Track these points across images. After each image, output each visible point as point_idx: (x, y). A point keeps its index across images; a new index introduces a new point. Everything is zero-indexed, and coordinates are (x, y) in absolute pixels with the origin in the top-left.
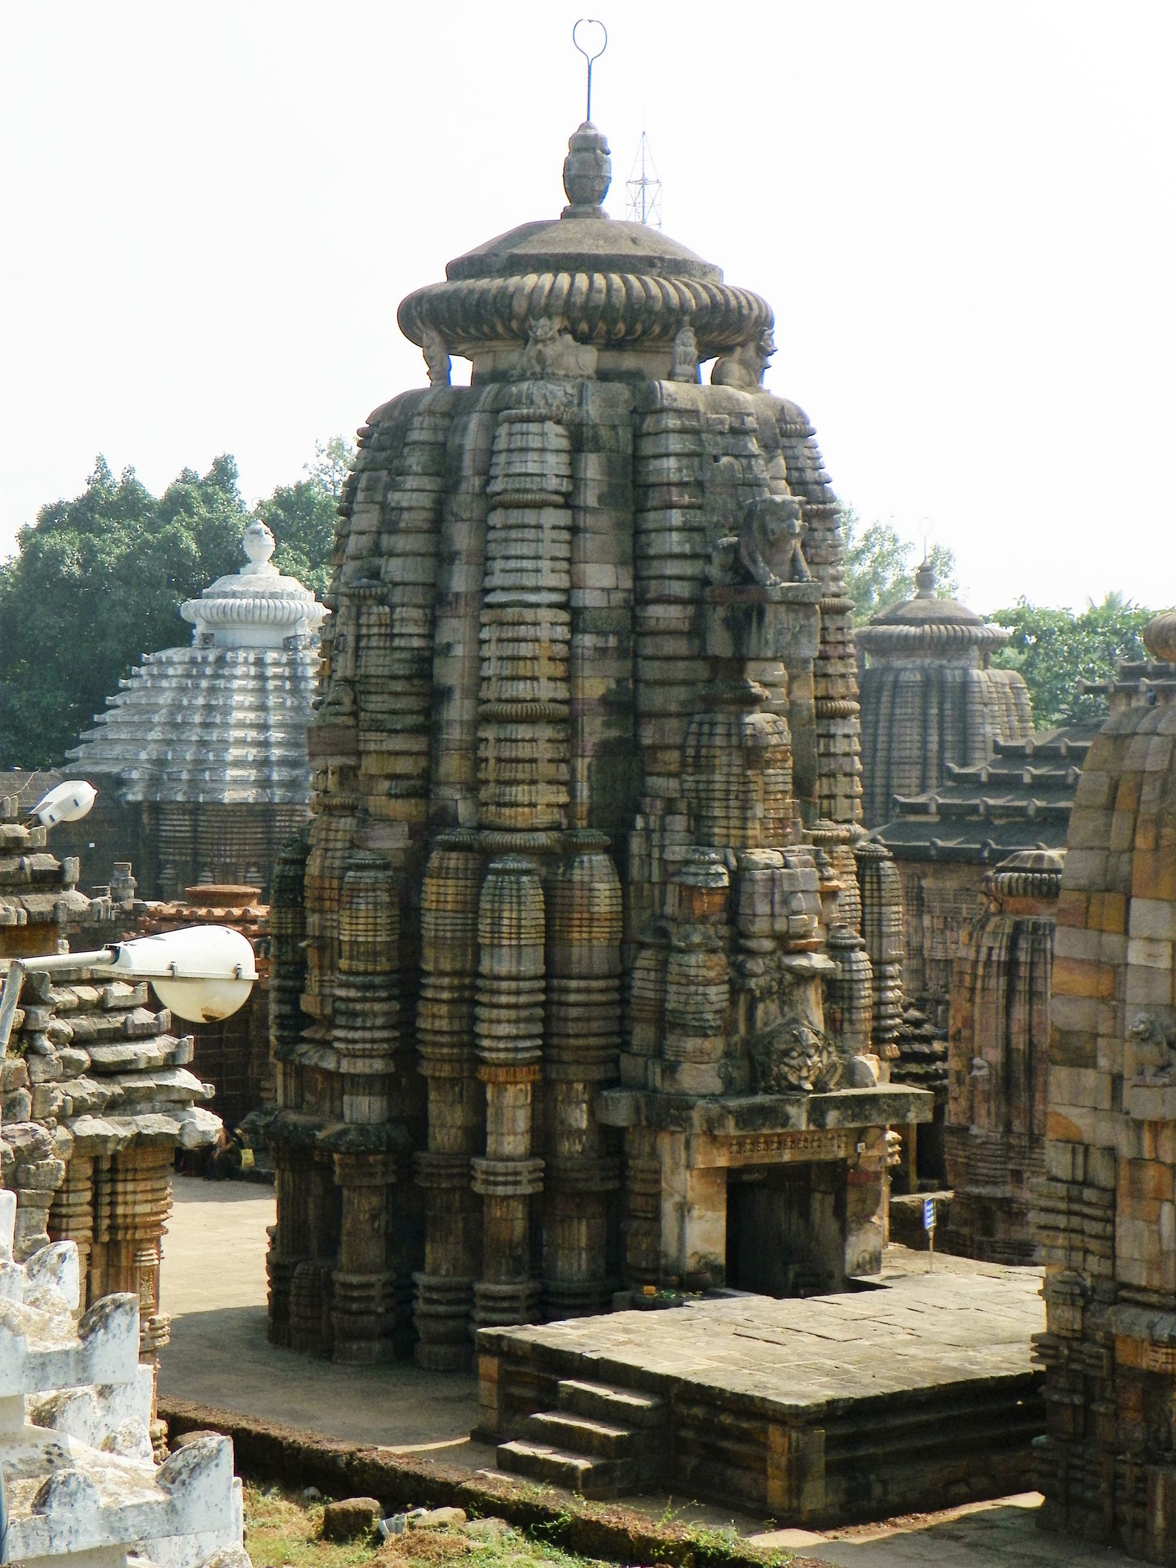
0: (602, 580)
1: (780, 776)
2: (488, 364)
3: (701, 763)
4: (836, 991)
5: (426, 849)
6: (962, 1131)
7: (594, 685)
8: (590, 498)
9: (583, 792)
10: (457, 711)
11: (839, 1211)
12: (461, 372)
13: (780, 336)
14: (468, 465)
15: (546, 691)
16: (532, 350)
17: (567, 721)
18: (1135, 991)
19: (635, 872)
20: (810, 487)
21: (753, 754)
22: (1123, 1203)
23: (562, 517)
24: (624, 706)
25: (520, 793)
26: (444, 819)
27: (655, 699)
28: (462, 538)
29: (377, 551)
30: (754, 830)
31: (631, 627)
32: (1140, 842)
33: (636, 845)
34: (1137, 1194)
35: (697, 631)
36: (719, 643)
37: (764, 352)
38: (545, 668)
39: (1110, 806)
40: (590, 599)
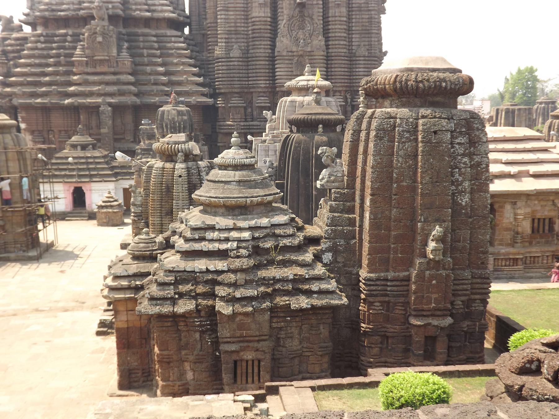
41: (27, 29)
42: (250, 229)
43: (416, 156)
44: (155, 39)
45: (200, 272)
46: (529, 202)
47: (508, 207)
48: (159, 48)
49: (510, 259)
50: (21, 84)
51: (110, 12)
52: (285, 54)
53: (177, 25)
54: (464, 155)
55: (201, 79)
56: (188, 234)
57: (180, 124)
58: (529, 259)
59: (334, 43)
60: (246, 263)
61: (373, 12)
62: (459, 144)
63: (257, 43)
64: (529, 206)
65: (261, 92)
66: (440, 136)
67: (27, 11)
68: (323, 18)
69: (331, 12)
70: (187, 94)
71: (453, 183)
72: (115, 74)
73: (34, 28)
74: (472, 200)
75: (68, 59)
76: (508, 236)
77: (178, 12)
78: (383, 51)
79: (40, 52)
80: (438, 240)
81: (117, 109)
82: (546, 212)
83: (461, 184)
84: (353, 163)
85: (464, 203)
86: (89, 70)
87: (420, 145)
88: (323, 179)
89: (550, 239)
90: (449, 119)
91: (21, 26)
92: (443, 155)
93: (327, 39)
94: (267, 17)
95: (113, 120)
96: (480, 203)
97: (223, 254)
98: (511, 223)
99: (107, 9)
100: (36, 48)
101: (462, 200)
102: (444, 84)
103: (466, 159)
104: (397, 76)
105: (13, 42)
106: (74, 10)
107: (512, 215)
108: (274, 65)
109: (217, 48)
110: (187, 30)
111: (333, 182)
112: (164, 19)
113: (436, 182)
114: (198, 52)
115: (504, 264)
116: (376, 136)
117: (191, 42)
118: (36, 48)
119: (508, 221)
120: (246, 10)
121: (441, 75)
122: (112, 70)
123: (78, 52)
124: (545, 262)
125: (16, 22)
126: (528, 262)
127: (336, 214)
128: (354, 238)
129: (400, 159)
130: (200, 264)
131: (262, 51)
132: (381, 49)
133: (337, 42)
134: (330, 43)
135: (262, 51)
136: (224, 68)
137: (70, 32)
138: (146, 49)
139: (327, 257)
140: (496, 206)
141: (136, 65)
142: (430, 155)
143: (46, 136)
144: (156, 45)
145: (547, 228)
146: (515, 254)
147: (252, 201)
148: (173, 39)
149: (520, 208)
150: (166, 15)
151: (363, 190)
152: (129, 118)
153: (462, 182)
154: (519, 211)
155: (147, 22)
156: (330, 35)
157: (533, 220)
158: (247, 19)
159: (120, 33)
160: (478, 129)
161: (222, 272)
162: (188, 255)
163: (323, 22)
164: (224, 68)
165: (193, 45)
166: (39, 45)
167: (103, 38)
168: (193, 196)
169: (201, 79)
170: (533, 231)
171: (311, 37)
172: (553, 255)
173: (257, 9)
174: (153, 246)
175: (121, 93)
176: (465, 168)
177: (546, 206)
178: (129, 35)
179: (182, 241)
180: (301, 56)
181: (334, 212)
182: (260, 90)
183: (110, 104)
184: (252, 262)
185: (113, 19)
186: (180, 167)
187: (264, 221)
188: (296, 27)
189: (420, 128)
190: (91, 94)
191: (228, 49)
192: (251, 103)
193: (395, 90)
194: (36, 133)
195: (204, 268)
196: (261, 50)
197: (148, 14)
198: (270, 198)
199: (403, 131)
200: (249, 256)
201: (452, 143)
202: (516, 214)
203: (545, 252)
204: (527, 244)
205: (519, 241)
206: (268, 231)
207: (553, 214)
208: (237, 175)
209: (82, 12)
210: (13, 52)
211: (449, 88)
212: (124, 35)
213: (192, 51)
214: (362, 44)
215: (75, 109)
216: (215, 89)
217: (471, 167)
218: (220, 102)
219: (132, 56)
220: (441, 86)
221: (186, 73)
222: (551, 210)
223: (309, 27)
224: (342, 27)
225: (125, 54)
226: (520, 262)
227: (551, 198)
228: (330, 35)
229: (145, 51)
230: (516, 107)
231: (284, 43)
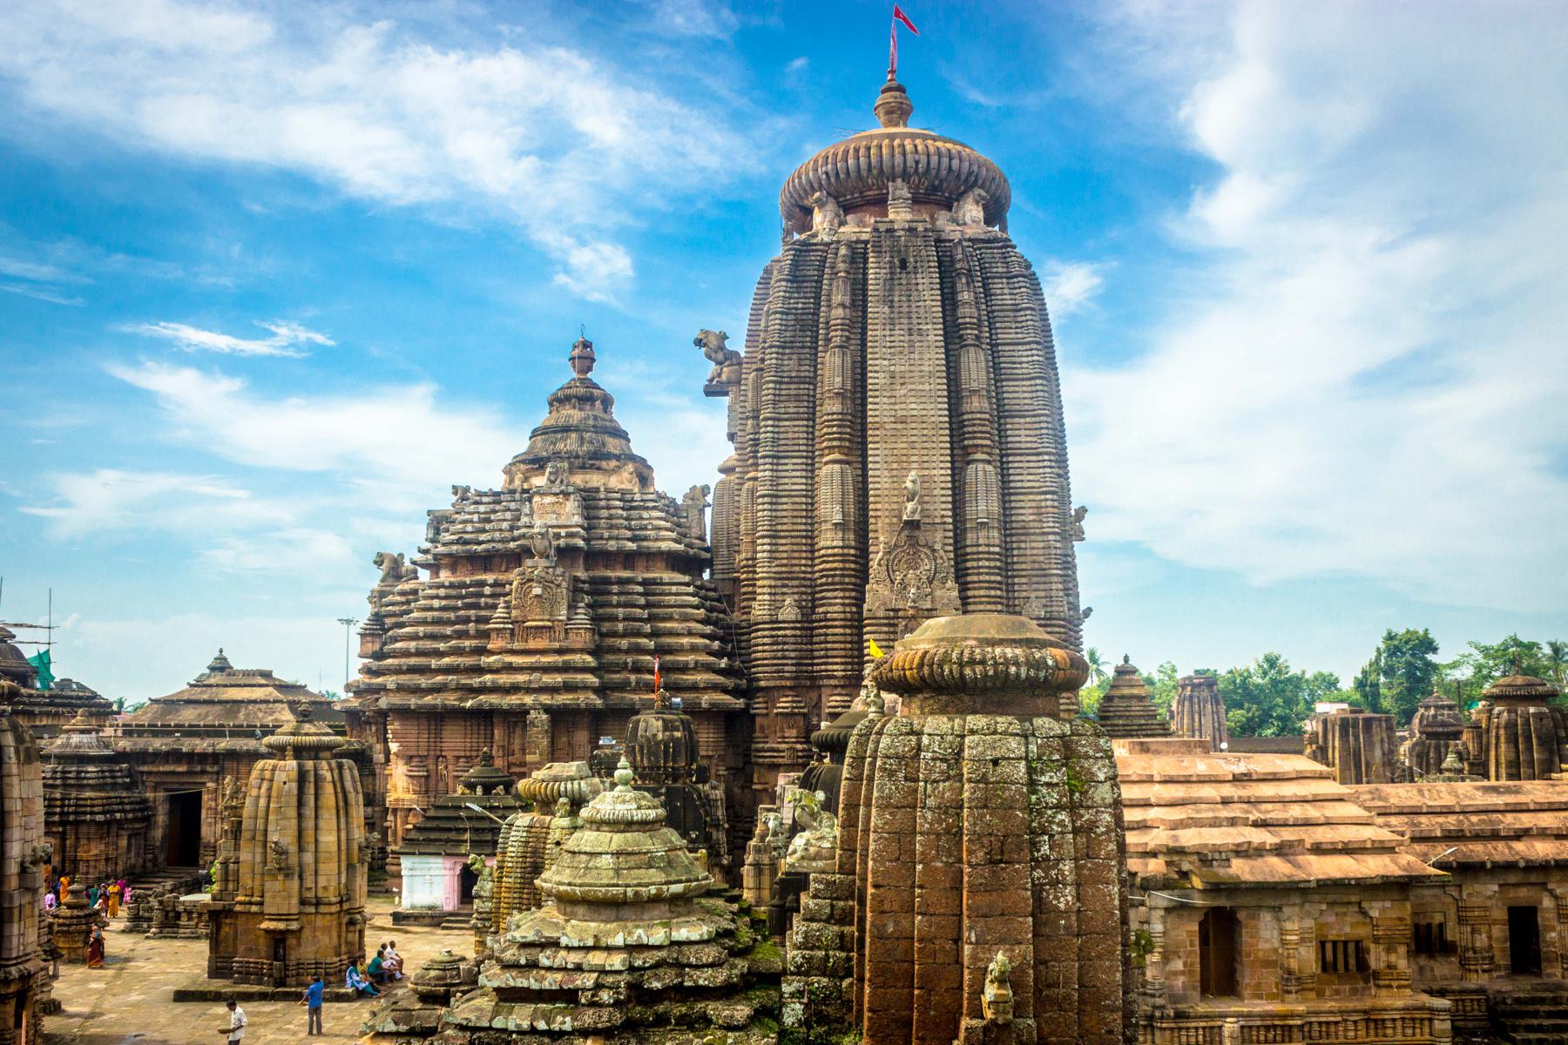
41: (424, 576)
42: (629, 948)
43: (961, 807)
44: (640, 589)
45: (518, 1033)
46: (1307, 906)
47: (1266, 917)
48: (648, 605)
49: (1275, 1027)
50: (398, 671)
51: (562, 542)
52: (881, 614)
53: (687, 563)
54: (1059, 807)
55: (724, 663)
56: (508, 956)
57: (667, 746)
58: (1316, 1027)
59: (976, 593)
60: (605, 1018)
61: (1051, 537)
62: (1048, 785)
63: (829, 594)
64: (1309, 914)
65: (836, 687)
66: (1005, 769)
67: (428, 545)
68: (956, 549)
69: (970, 538)
70: (694, 688)
71: (1037, 863)
72: (560, 652)
73: (436, 573)
74: (1078, 898)
75: (482, 627)
76: (1271, 978)
77: (687, 540)
78: (1082, 607)
79: (436, 614)
80: (1001, 981)
81: (561, 718)
82: (1345, 927)
83: (1056, 866)
84: (849, 824)
85: (1062, 906)
86: (516, 646)
87: (966, 786)
88: (795, 852)
89: (1361, 985)
90: (1026, 737)
91: (415, 572)
92: (1011, 808)
93: (963, 587)
94: (849, 547)
95: (553, 738)
96: (1098, 906)
97: (568, 997)
98: (1276, 950)
99: (557, 536)
100: (431, 609)
101: (1057, 898)
102: (1013, 669)
103: (1063, 816)
104: (926, 652)
105: (398, 598)
106: (502, 541)
107: (1276, 933)
108: (861, 634)
109: (755, 604)
110: (706, 575)
111: (814, 859)
112: (661, 554)
113: (1001, 861)
114: (724, 612)
115: (1262, 1038)
116: (883, 769)
117: (711, 594)
118: (431, 609)
119: (1267, 946)
120: (811, 537)
121: (1009, 652)
122: (556, 645)
123: (500, 612)
124: (1351, 1034)
125: (407, 563)
126: (1315, 1034)
127: (814, 925)
128: (850, 975)
129: (929, 815)
130: (519, 1017)
131: (836, 608)
132: (1074, 607)
133: (982, 592)
134: (970, 593)
135: (836, 608)
136: (766, 640)
137: (491, 581)
138: (625, 605)
139: (793, 1013)
140: (1241, 915)
141: (602, 635)
142: (985, 806)
143: (432, 767)
144: (642, 601)
145: (1352, 961)
146: (1285, 1017)
147: (636, 893)
148: (674, 589)
149: (1289, 919)
150: (665, 546)
151: (864, 880)
152: (582, 736)
153: (1058, 861)
154: (1289, 926)
155: (629, 559)
156: (969, 579)
157: (1323, 944)
158: (812, 552)
159: (576, 579)
160: (1087, 757)
161: (562, 1033)
162: (508, 996)
163: (956, 556)
164: (766, 640)
165: (712, 600)
166: (436, 603)
167: (544, 588)
168: (537, 882)
169: (724, 663)
170: (1324, 969)
171: (931, 583)
172: (1367, 1020)
173: (829, 535)
174: (452, 977)
175: (569, 688)
176: (1062, 833)
177: (1345, 914)
178: (593, 581)
179: (497, 969)
180: (913, 617)
181: (812, 920)
182: (833, 682)
183: (548, 709)
184: (618, 1018)
185: (566, 554)
186: (560, 822)
187: (658, 936)
188: (903, 566)
189: (966, 753)
190: (514, 689)
191: (776, 606)
192: (818, 705)
193: (922, 678)
194: (415, 762)
195: (525, 1025)
196: (834, 606)
197: (631, 546)
198: (677, 888)
199: (933, 759)
200: (617, 1004)
201: (1032, 784)
202: (1282, 932)
203: (1349, 1012)
204: (1313, 995)
205: (1293, 989)
206: (663, 954)
207: (1363, 931)
208: (618, 840)
209: (512, 545)
210: (394, 615)
211: (1023, 675)
212: (584, 582)
213: (711, 610)
214: (1033, 595)
215: (484, 718)
216: (750, 681)
217: (1076, 831)
218: (759, 706)
219: (596, 619)
220: (1008, 674)
221: (694, 649)
222: (1357, 924)
223: (926, 565)
224: (992, 564)
225: (582, 616)
226: (1296, 1034)
227: (1354, 899)
228: (969, 579)
229: (621, 612)
230: (1361, 716)
231: (878, 595)
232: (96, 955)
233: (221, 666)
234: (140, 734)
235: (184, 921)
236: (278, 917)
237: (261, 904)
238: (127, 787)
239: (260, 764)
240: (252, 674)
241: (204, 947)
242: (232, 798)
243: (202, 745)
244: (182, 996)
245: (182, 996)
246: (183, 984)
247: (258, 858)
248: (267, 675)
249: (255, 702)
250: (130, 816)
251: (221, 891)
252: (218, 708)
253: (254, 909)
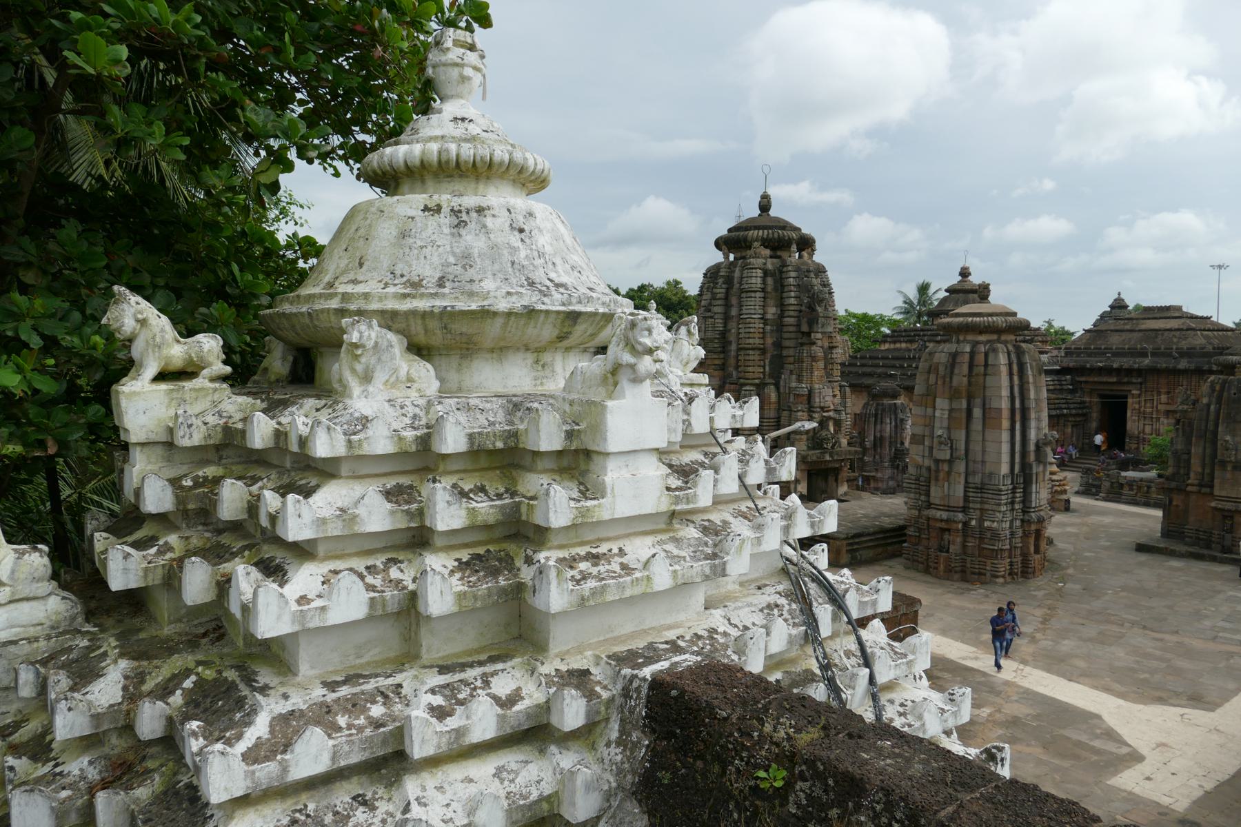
0: (772, 311)
1: (821, 364)
2: (739, 255)
3: (800, 361)
4: (838, 423)
5: (724, 383)
6: (861, 459)
7: (769, 341)
8: (769, 289)
9: (767, 368)
10: (733, 347)
11: (836, 480)
12: (732, 257)
13: (817, 245)
14: (736, 281)
15: (757, 341)
16: (752, 251)
17: (763, 351)
18: (937, 424)
19: (782, 390)
20: (826, 284)
21: (814, 359)
22: (933, 482)
23: (762, 295)
24: (778, 345)
25: (750, 369)
26: (730, 375)
27: (786, 343)
28: (734, 301)
29: (710, 304)
30: (815, 378)
31: (779, 325)
32: (939, 382)
33: (782, 383)
34: (937, 479)
35: (798, 325)
36: (805, 328)
37: (813, 250)
38: (757, 335)
39: (929, 372)
40: (769, 316)
232: (1067, 507)
233: (1119, 305)
234: (1078, 355)
235: (1125, 491)
236: (1228, 499)
237: (1212, 487)
238: (1072, 392)
239: (1212, 378)
240: (1168, 308)
241: (1159, 513)
242: (1182, 403)
243: (1127, 362)
244: (1141, 548)
245: (1141, 548)
246: (1143, 540)
247: (1208, 451)
248: (1179, 308)
249: (1170, 330)
250: (1074, 412)
251: (1174, 474)
252: (1136, 335)
253: (1206, 490)
